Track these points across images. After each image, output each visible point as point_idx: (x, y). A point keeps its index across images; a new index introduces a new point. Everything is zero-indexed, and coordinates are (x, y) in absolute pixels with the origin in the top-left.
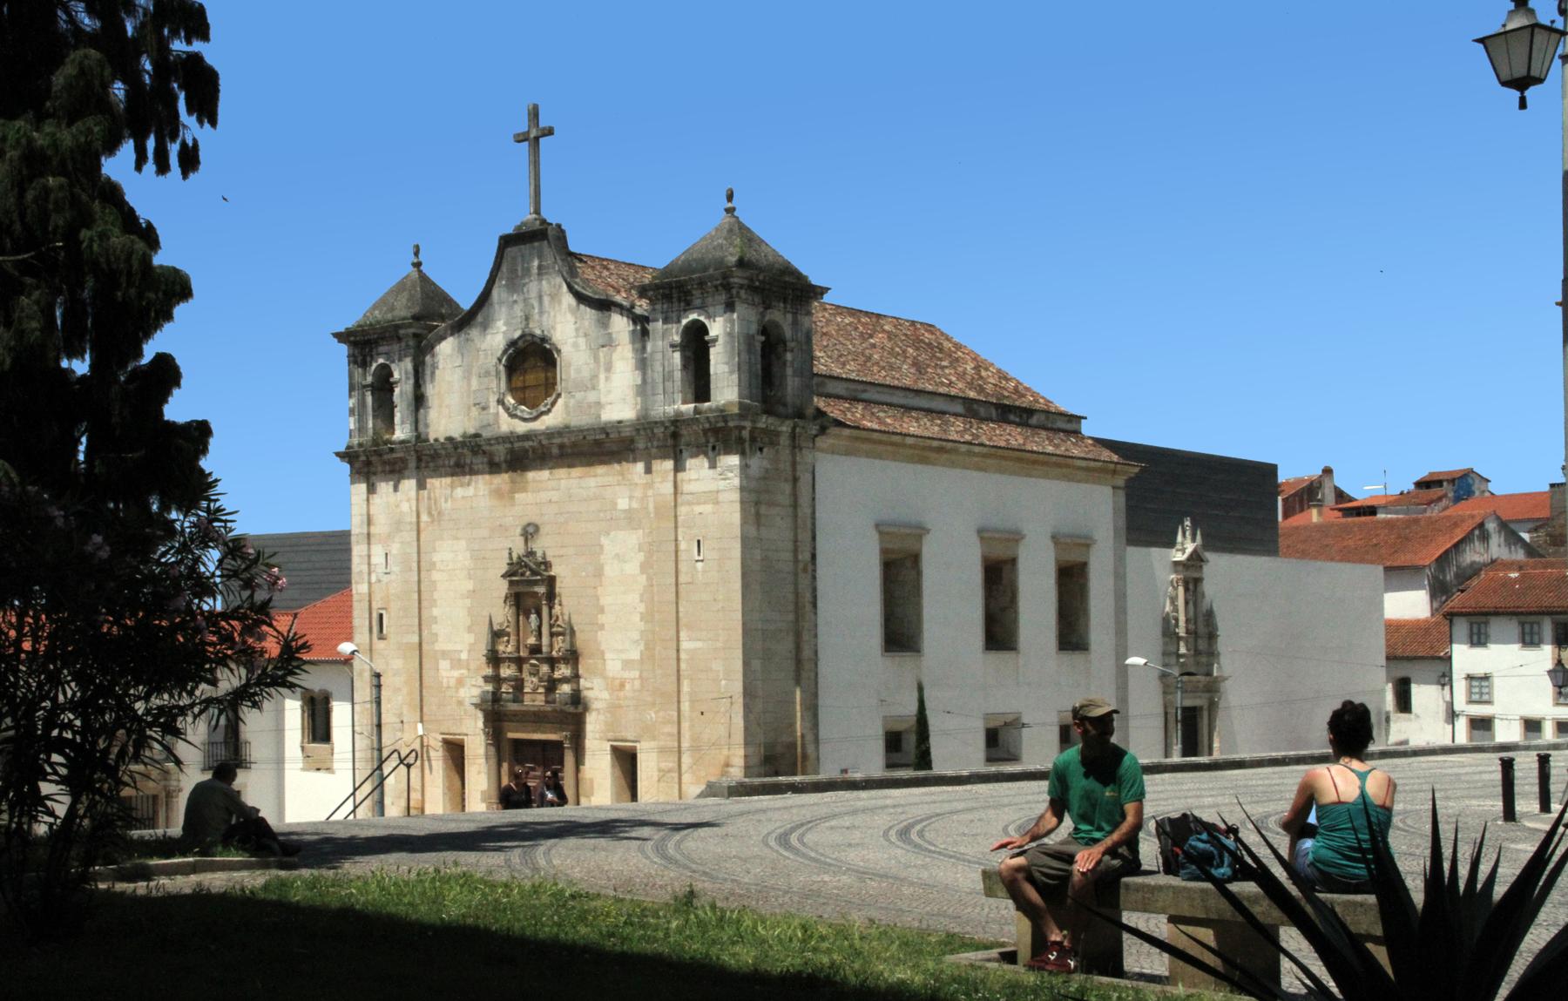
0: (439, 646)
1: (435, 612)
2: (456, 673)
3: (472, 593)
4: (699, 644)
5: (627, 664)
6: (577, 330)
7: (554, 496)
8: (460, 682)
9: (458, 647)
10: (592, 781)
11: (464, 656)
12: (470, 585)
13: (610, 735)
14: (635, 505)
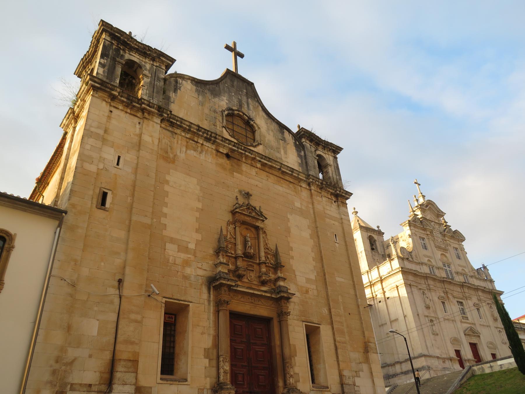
0: (169, 232)
1: (165, 210)
2: (183, 256)
3: (198, 210)
4: (342, 280)
5: (308, 280)
6: (267, 126)
7: (260, 185)
8: (186, 263)
9: (187, 239)
10: (294, 345)
11: (192, 246)
12: (200, 206)
13: (303, 318)
14: (303, 208)
